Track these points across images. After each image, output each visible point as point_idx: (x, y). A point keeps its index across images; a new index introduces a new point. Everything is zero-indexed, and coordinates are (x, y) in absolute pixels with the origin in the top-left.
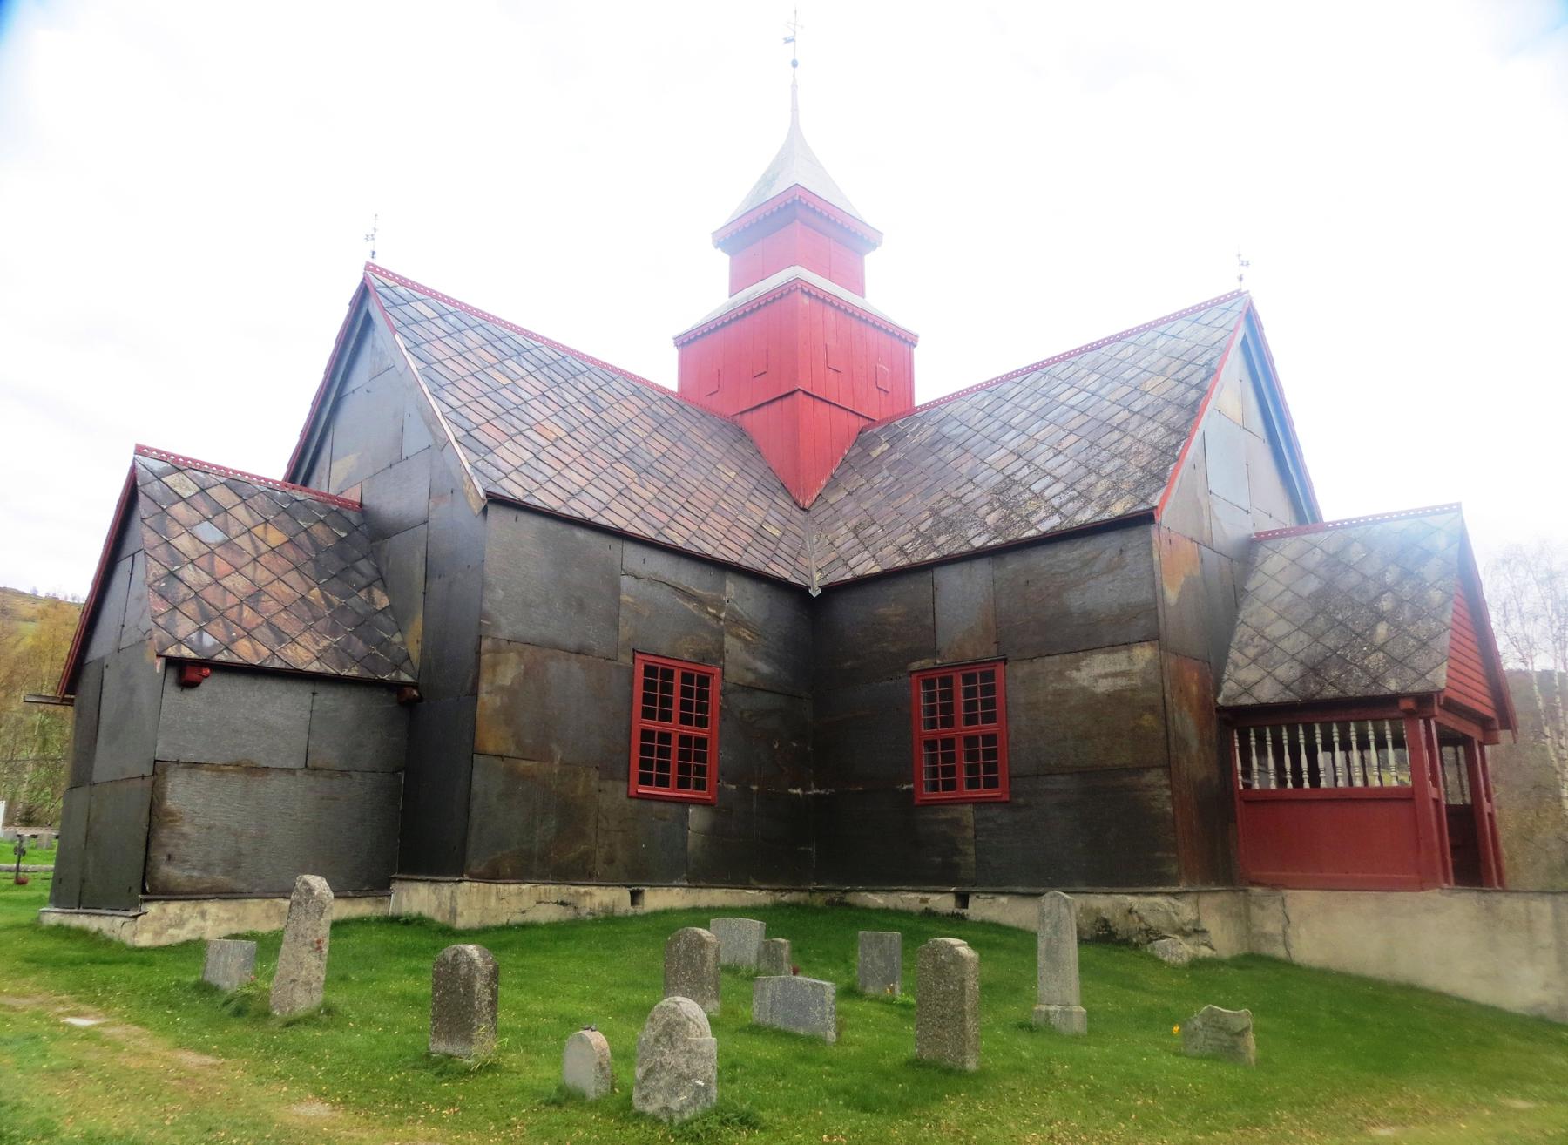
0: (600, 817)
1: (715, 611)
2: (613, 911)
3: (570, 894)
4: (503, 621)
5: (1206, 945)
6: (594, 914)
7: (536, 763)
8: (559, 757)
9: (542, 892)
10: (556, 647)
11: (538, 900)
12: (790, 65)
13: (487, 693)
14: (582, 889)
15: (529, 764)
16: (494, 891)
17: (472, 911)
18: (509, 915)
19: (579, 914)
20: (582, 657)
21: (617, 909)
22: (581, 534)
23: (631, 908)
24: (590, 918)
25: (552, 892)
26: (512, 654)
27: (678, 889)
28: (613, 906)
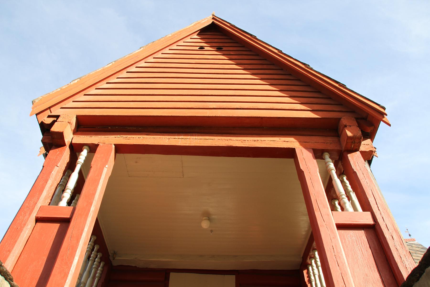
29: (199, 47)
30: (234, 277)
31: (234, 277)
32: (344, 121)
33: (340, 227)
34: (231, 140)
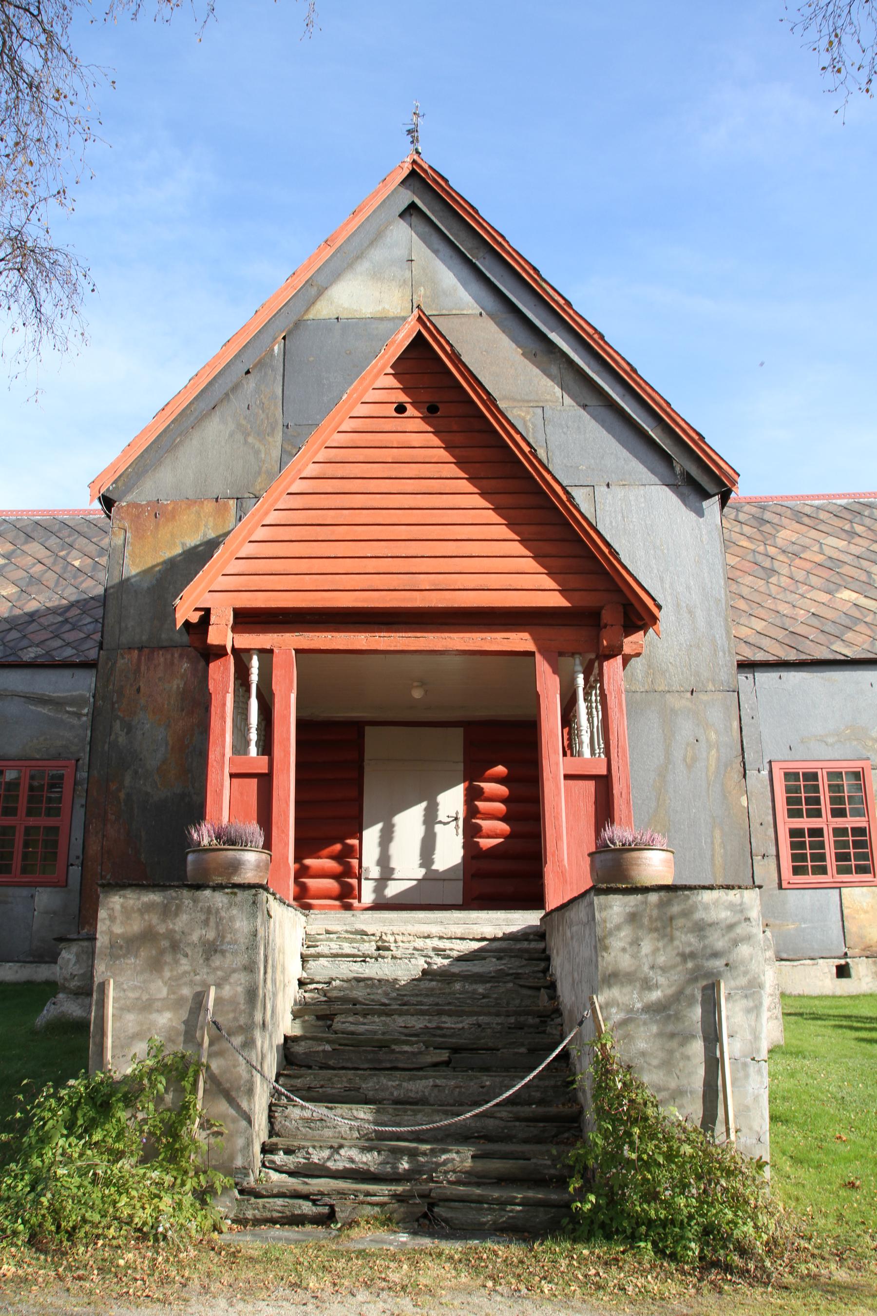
1: (75, 709)
29: (395, 405)
30: (460, 731)
31: (460, 731)
32: (607, 616)
33: (567, 777)
34: (450, 638)
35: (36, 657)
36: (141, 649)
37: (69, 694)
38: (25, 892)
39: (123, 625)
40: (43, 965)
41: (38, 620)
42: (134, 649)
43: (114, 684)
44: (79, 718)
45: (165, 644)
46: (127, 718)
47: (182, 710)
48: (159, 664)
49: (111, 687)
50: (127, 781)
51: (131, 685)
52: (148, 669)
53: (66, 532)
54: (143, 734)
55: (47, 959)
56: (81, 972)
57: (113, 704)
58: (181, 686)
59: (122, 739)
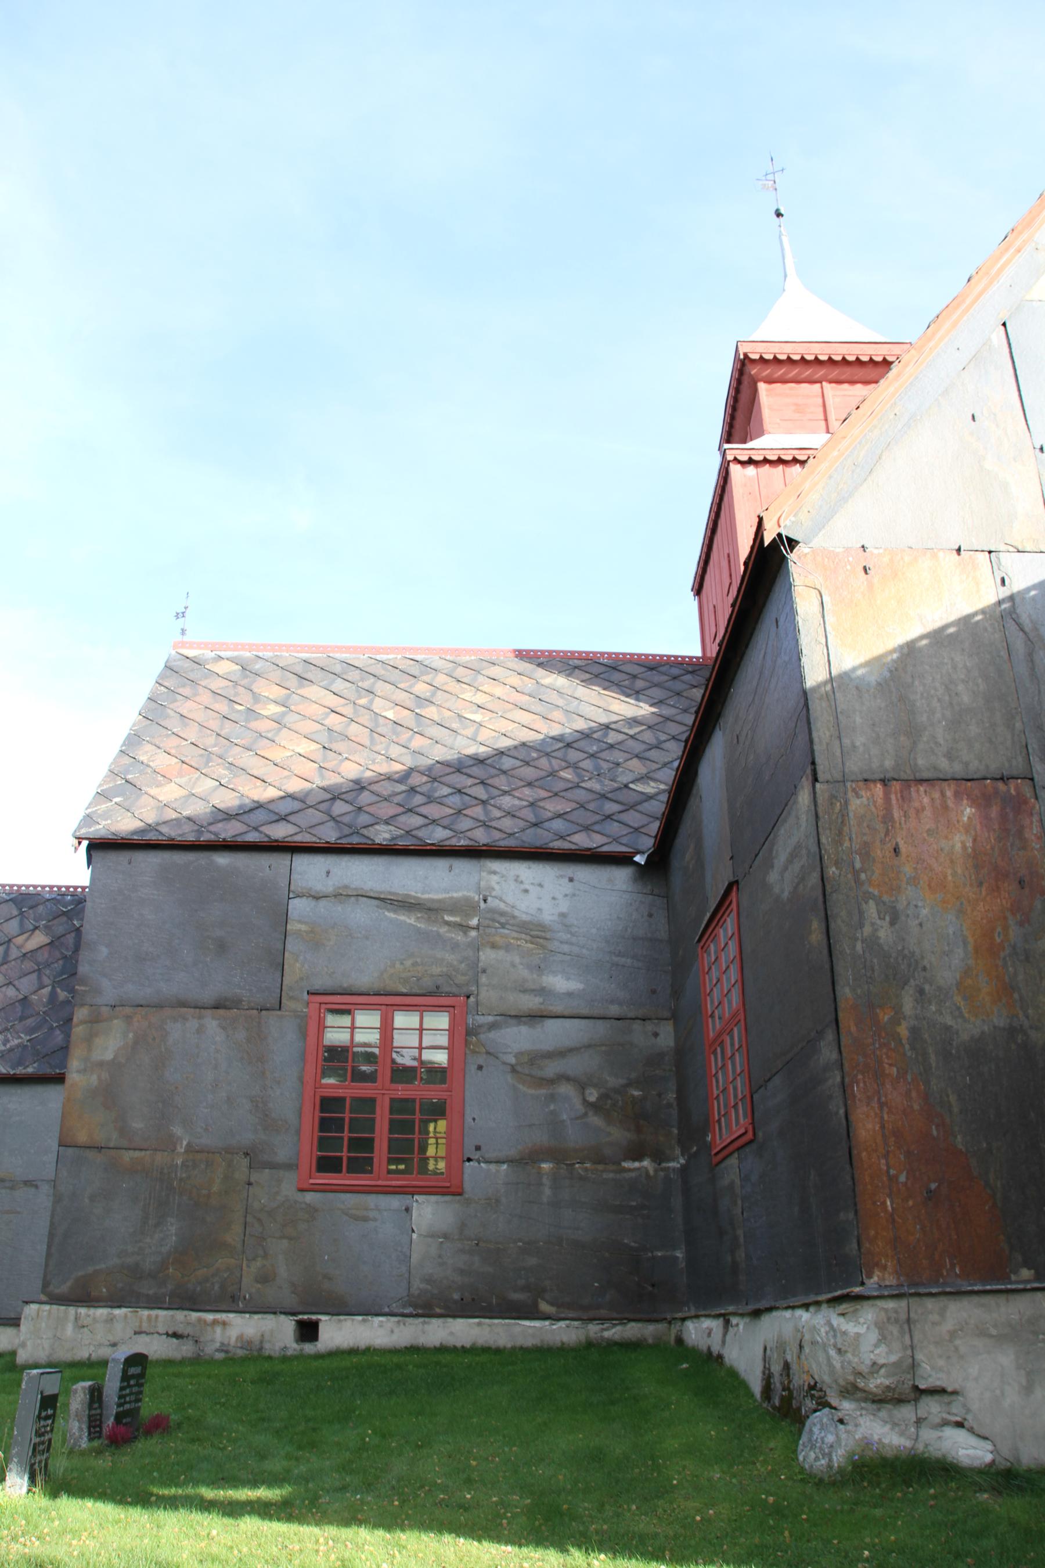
0: (249, 1219)
1: (457, 919)
2: (261, 1349)
3: (189, 1324)
4: (105, 983)
5: (960, 1425)
6: (227, 1352)
7: (148, 1152)
8: (185, 1143)
9: (145, 1318)
10: (183, 1004)
11: (137, 1330)
12: (775, 216)
13: (78, 1071)
14: (210, 1317)
15: (137, 1154)
16: (72, 1317)
17: (39, 1341)
18: (92, 1348)
19: (203, 1351)
20: (221, 1012)
21: (267, 1346)
22: (222, 860)
23: (295, 1345)
24: (220, 1356)
25: (160, 1319)
26: (115, 1021)
27: (381, 1319)
28: (261, 1342)
35: (393, 839)
36: (884, 781)
37: (447, 896)
38: (395, 1202)
39: (846, 742)
40: (434, 1321)
41: (369, 787)
42: (874, 781)
43: (850, 839)
44: (465, 933)
45: (926, 775)
46: (885, 898)
47: (980, 884)
48: (923, 809)
49: (847, 844)
50: (908, 1005)
51: (883, 842)
52: (906, 815)
53: (353, 675)
54: (921, 925)
55: (438, 1310)
56: (893, 1358)
57: (856, 873)
58: (969, 844)
59: (885, 934)
